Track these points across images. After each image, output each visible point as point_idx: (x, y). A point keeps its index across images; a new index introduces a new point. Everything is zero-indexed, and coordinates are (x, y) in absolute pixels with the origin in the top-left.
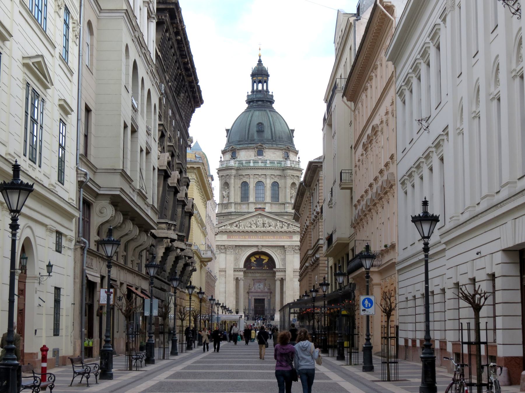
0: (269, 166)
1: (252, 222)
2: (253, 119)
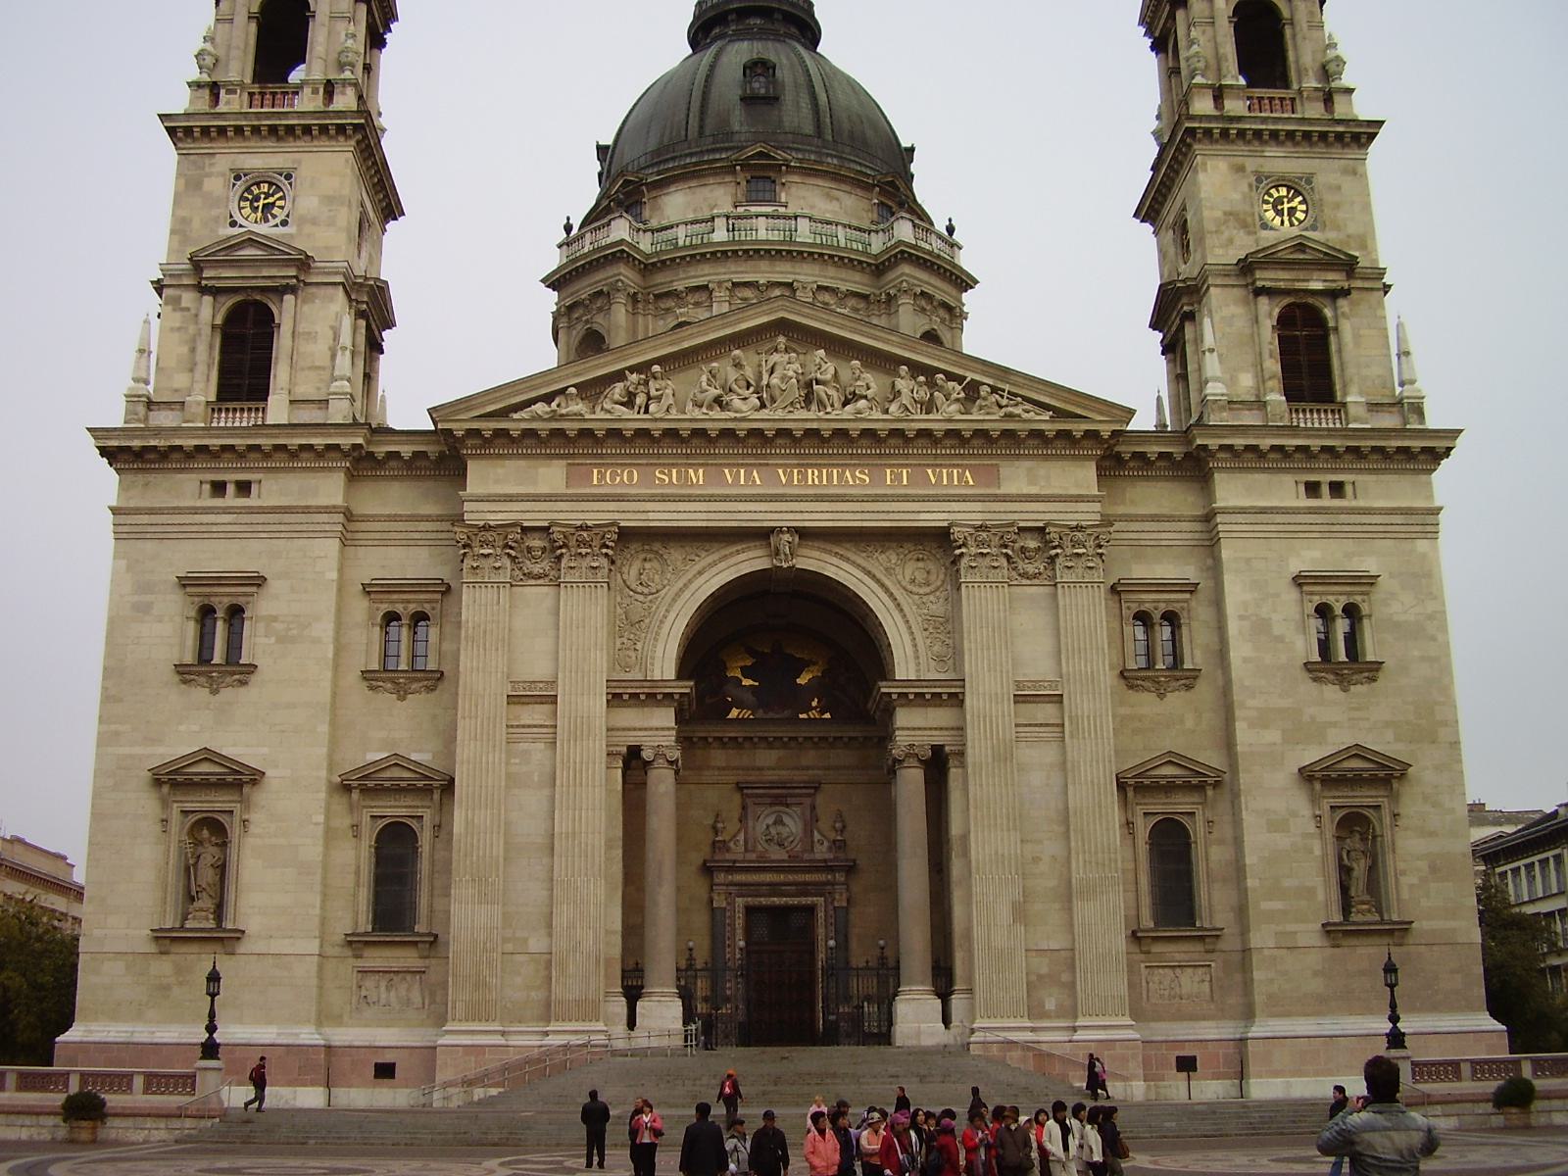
2: (724, 59)
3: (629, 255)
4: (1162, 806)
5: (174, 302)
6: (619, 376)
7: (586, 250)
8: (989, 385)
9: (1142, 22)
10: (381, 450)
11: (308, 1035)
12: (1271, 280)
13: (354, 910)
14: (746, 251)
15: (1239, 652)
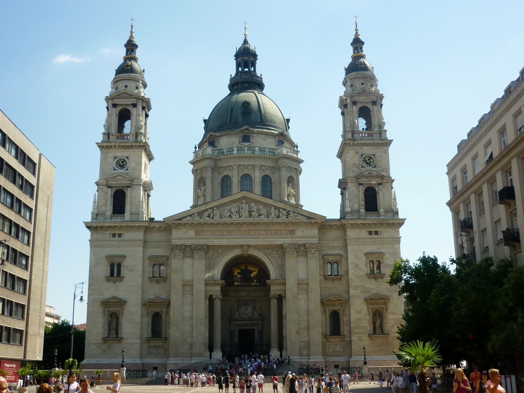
0: (259, 153)
1: (233, 210)
3: (211, 158)
4: (332, 308)
5: (102, 189)
6: (207, 210)
7: (200, 155)
8: (292, 211)
9: (339, 107)
10: (152, 226)
11: (138, 361)
12: (363, 181)
13: (148, 333)
14: (242, 157)
15: (351, 272)
